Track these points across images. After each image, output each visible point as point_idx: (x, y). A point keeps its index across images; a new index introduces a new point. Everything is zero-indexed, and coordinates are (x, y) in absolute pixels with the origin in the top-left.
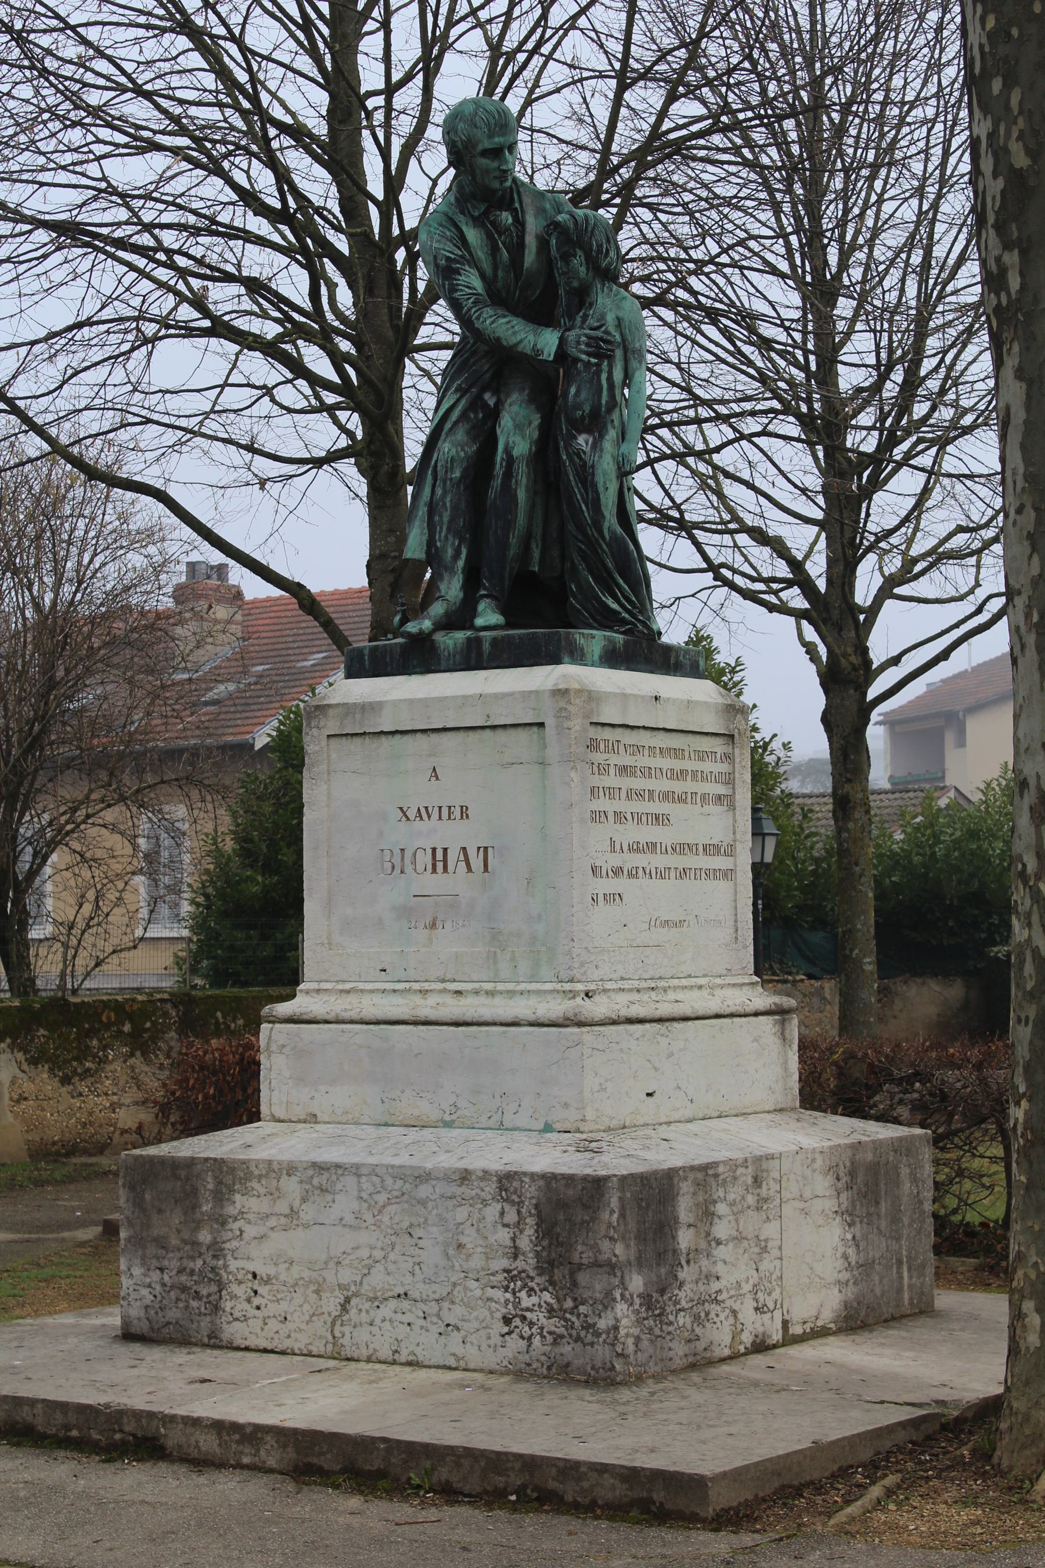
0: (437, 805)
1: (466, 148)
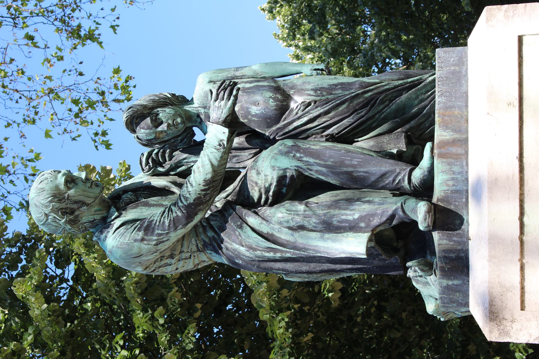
1: (60, 201)
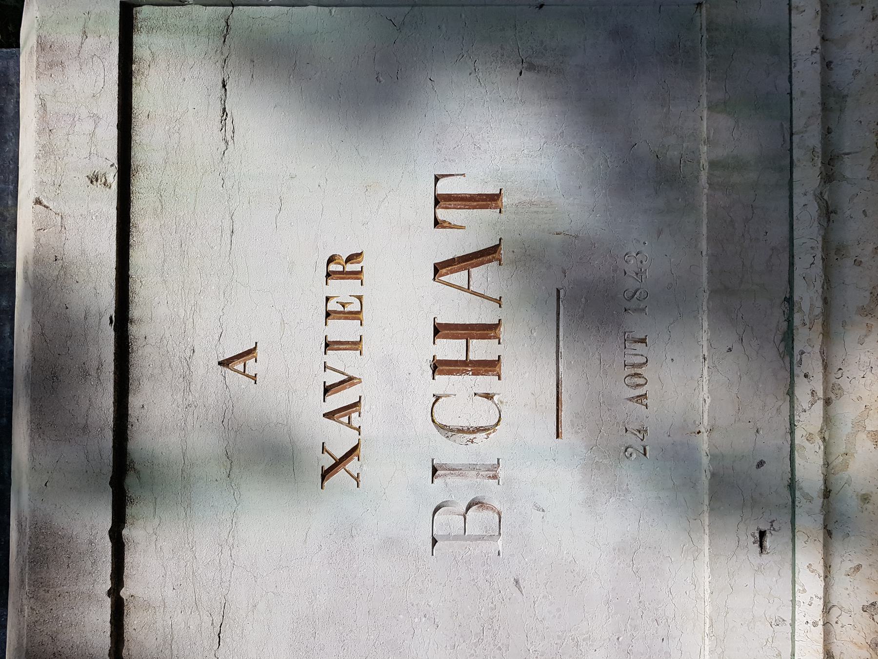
0: (318, 354)
